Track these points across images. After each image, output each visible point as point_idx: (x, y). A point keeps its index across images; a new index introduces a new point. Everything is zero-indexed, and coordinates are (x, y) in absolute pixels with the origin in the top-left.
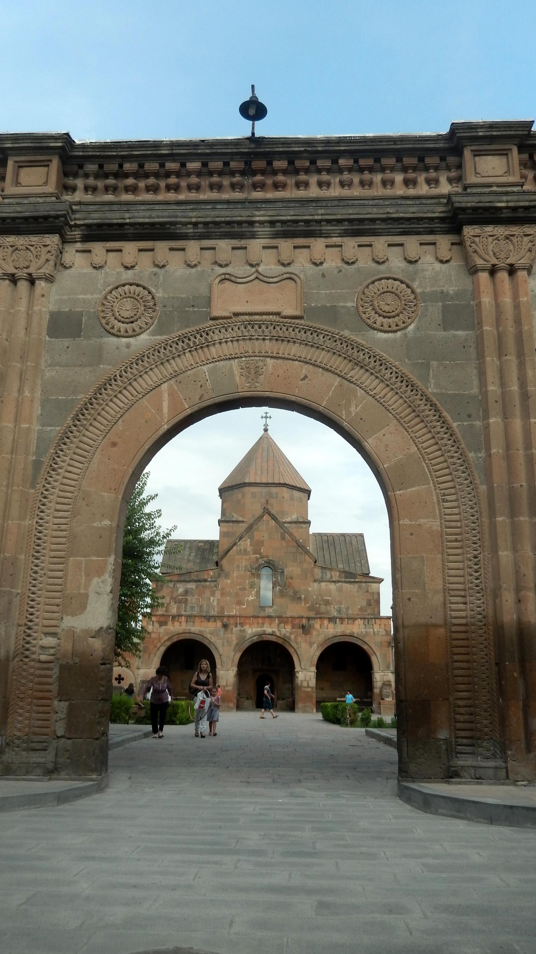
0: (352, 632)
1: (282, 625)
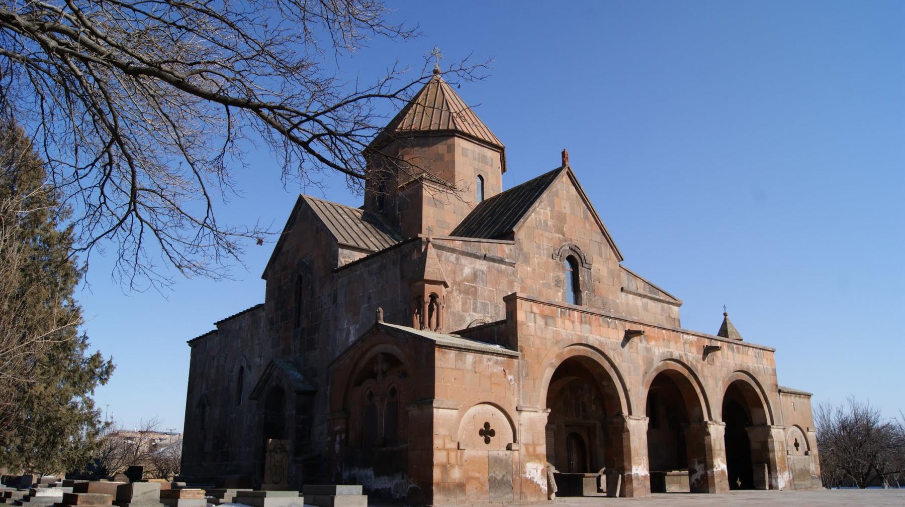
0: (748, 365)
1: (687, 346)
